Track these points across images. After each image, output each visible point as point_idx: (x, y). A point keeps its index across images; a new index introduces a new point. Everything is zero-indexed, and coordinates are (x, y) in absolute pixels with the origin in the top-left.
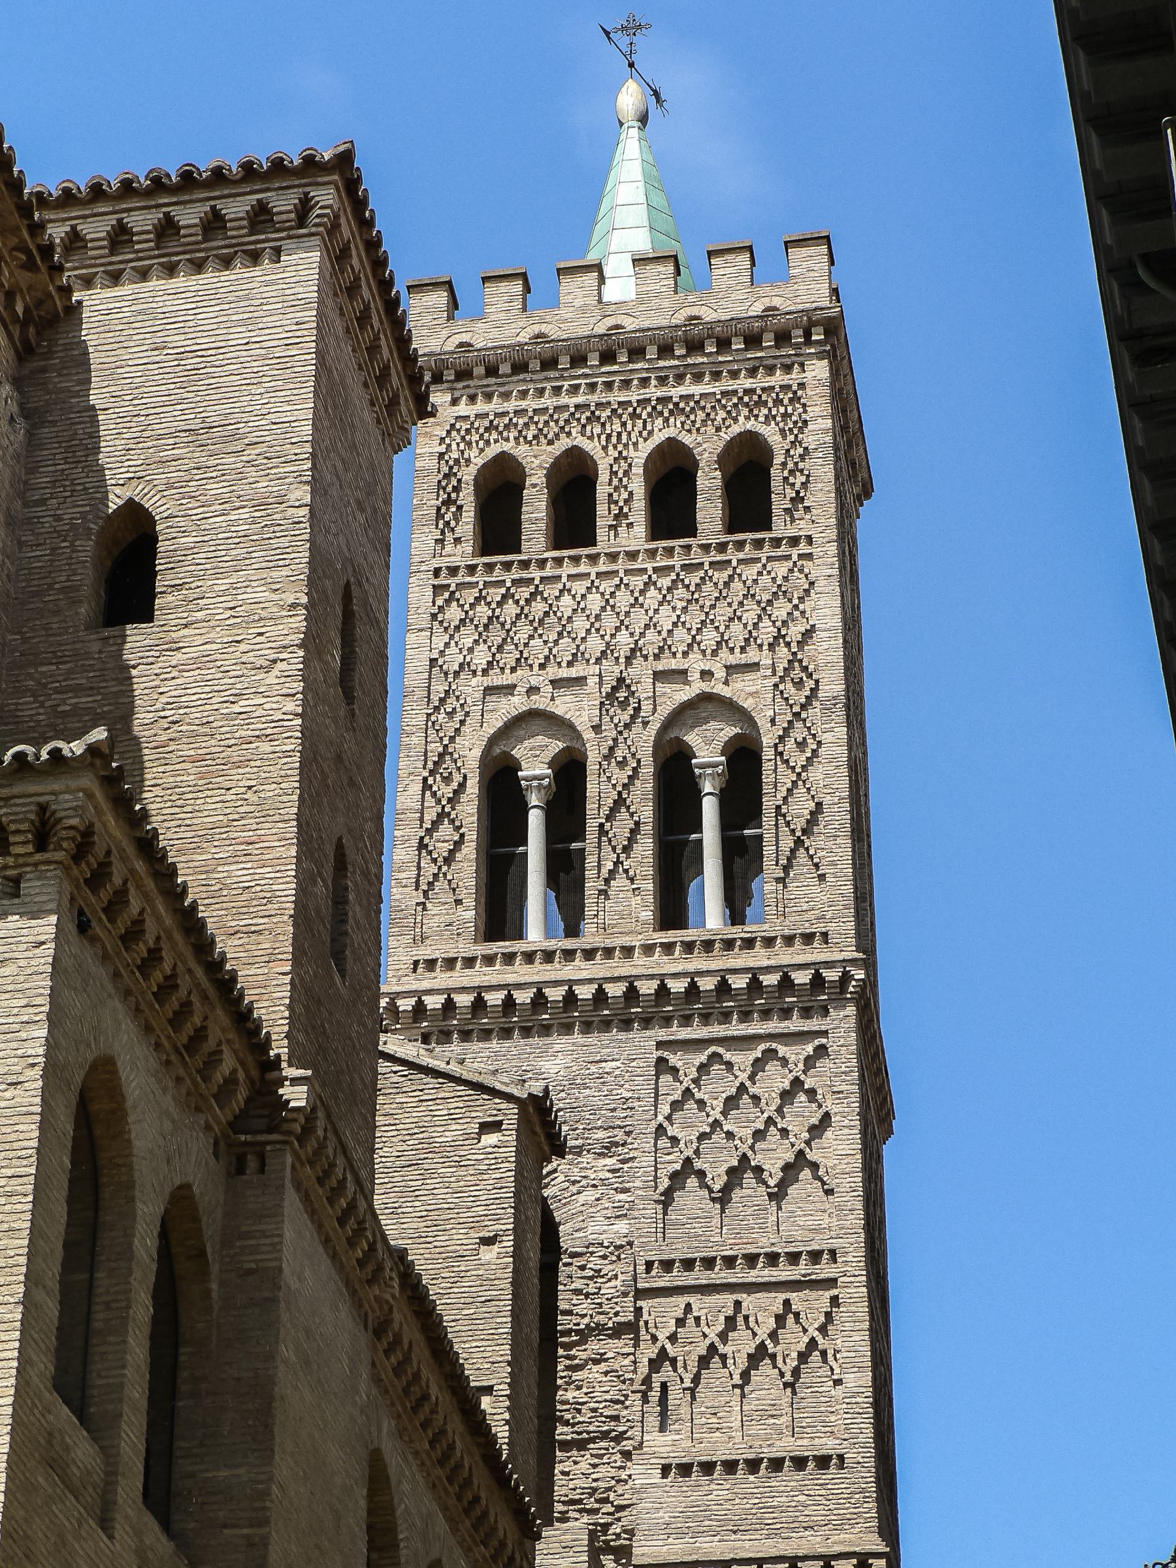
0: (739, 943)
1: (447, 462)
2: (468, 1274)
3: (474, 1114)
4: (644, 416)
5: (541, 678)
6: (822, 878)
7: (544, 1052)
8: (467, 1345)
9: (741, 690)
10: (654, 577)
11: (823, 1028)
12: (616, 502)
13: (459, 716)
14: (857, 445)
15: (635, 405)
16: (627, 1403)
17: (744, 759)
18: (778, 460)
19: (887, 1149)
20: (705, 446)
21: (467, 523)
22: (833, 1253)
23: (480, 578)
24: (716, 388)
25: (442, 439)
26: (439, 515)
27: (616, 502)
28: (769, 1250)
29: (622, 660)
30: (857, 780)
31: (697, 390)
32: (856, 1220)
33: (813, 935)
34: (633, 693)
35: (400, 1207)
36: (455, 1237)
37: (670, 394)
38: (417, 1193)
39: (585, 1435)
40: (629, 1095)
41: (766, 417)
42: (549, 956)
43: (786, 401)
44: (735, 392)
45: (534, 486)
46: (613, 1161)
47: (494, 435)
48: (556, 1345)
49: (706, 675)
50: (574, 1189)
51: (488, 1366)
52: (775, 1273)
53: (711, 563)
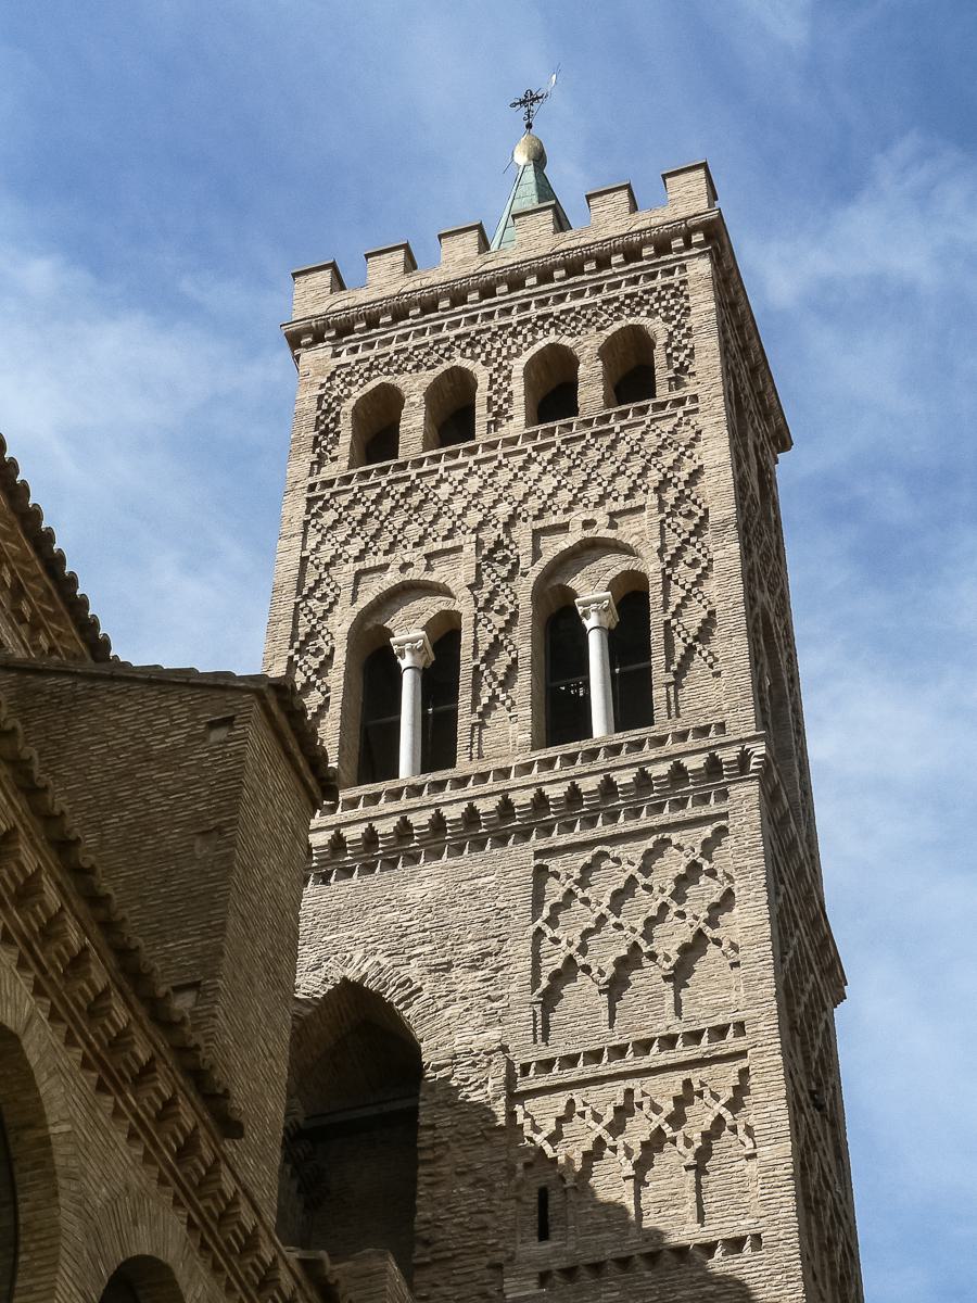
0: (625, 747)
1: (326, 401)
4: (524, 331)
6: (717, 674)
7: (409, 880)
9: (627, 532)
10: (534, 454)
11: (723, 810)
12: (496, 403)
16: (499, 1213)
17: (631, 598)
18: (661, 340)
19: (841, 1014)
20: (586, 343)
21: (345, 444)
22: (740, 1028)
23: (355, 485)
24: (598, 299)
25: (322, 386)
26: (316, 443)
27: (496, 403)
28: (665, 1033)
32: (767, 989)
34: (512, 551)
35: (104, 820)
37: (550, 311)
38: (126, 802)
39: (449, 1254)
40: (505, 904)
41: (648, 311)
42: (416, 791)
44: (616, 299)
45: (413, 404)
46: (487, 971)
47: (375, 373)
48: (416, 1164)
49: (588, 524)
50: (440, 1004)
52: (673, 1055)
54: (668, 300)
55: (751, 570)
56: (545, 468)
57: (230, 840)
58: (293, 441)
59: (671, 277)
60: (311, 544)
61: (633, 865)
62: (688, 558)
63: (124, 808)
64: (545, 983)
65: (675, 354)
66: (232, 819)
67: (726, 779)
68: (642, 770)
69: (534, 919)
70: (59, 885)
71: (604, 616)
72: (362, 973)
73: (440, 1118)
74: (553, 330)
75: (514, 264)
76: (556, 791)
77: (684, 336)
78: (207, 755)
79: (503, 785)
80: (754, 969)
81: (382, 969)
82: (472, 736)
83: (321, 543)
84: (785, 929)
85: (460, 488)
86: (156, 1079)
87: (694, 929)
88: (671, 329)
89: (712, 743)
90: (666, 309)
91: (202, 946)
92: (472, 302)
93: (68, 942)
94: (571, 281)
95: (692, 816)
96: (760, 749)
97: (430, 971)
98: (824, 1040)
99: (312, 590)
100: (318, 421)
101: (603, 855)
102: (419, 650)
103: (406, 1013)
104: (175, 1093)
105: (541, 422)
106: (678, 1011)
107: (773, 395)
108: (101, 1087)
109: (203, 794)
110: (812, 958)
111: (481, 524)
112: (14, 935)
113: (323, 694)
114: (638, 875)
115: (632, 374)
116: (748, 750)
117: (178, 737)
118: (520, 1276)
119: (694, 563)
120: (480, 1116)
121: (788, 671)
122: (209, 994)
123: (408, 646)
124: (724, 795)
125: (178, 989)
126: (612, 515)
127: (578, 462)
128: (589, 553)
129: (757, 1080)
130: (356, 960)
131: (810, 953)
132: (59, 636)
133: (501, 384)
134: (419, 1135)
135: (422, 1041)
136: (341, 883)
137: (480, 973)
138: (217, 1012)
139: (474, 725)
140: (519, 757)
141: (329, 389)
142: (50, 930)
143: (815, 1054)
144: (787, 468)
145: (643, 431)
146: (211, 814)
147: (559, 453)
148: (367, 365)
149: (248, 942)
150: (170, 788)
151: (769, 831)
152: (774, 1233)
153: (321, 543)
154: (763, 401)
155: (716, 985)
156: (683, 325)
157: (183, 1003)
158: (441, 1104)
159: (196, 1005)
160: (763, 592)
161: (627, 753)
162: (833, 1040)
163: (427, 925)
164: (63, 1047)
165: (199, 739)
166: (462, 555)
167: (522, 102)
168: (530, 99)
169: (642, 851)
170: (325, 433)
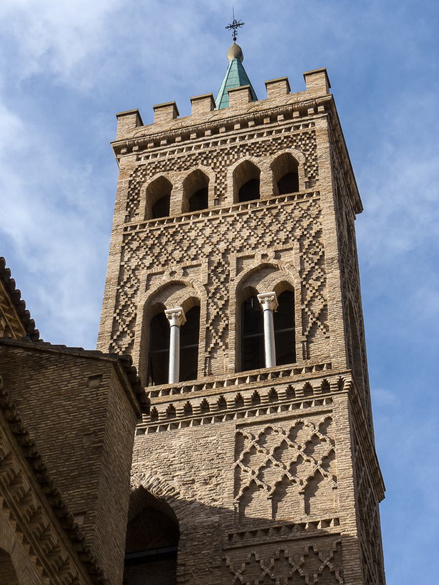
0: (281, 373)
2: (76, 454)
4: (233, 153)
5: (178, 267)
6: (329, 337)
8: (72, 492)
10: (238, 218)
11: (330, 409)
12: (218, 190)
13: (135, 288)
14: (350, 179)
15: (229, 149)
17: (285, 294)
18: (302, 161)
19: (383, 507)
21: (142, 207)
22: (337, 521)
23: (147, 229)
24: (270, 138)
25: (131, 175)
26: (128, 206)
27: (218, 190)
28: (300, 522)
29: (220, 254)
30: (352, 318)
31: (260, 139)
32: (351, 502)
33: (323, 365)
35: (37, 425)
36: (69, 436)
37: (246, 143)
38: (48, 416)
41: (296, 146)
42: (177, 391)
43: (306, 139)
44: (280, 138)
45: (177, 188)
46: (212, 486)
49: (264, 256)
51: (84, 501)
52: (304, 534)
53: (268, 209)
54: (306, 141)
55: (344, 283)
56: (243, 225)
57: (100, 439)
58: (116, 204)
59: (307, 128)
60: (126, 259)
61: (285, 434)
62: (314, 277)
63: (48, 419)
64: (241, 493)
65: (309, 169)
66: (101, 428)
67: (332, 393)
68: (290, 386)
69: (235, 460)
70: (29, 478)
71: (272, 304)
72: (150, 484)
73: (187, 561)
74: (247, 153)
75: (229, 118)
76: (248, 395)
77: (314, 160)
78: (89, 394)
79: (221, 390)
80: (344, 491)
81: (160, 482)
82: (205, 364)
83: (131, 257)
84: (358, 468)
85: (200, 234)
86: (69, 568)
87: (315, 469)
88: (307, 156)
89: (325, 374)
90: (305, 145)
91: (87, 493)
92: (207, 136)
93: (33, 505)
94: (257, 127)
95: (315, 411)
96: (348, 379)
97: (184, 485)
98: (375, 521)
99: (126, 283)
100: (129, 195)
101: (270, 428)
102: (179, 317)
103: (172, 505)
104: (77, 574)
105: (240, 201)
106: (307, 510)
107: (355, 186)
108: (44, 574)
109: (87, 414)
110: (370, 479)
111: (210, 253)
112: (8, 504)
113: (131, 337)
114: (287, 440)
115: (287, 179)
116: (343, 378)
117: (74, 384)
119: (318, 279)
120: (208, 560)
121: (360, 330)
122: (90, 518)
123: (173, 314)
124: (330, 401)
125: (76, 515)
126: (276, 252)
127: (259, 223)
128: (264, 271)
129: (345, 549)
130: (147, 476)
131: (369, 477)
132: (10, 320)
133: (221, 180)
134: (177, 569)
135: (179, 520)
136: (139, 436)
137: (208, 486)
138: (94, 528)
139: (206, 358)
140: (229, 376)
141: (135, 177)
142: (23, 500)
143: (371, 531)
144: (360, 224)
145: (291, 208)
146: (90, 425)
147: (250, 217)
148: (153, 166)
149: (108, 490)
150: (70, 410)
151: (352, 419)
153: (131, 257)
154: (349, 189)
155: (325, 498)
156: (313, 154)
157: (79, 521)
158: (188, 554)
159: (84, 524)
160: (349, 291)
161: (283, 376)
162: (379, 520)
163: (182, 460)
164: (28, 557)
165: (85, 385)
166: (201, 268)
167: (232, 26)
168: (235, 25)
169: (289, 427)
170: (132, 201)
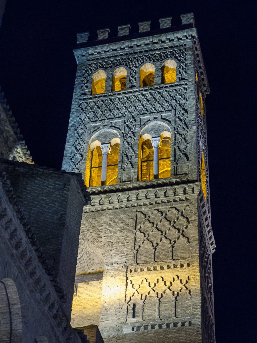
3: (57, 183)
78: (58, 194)
118: (127, 327)
150: (48, 202)
152: (195, 321)
